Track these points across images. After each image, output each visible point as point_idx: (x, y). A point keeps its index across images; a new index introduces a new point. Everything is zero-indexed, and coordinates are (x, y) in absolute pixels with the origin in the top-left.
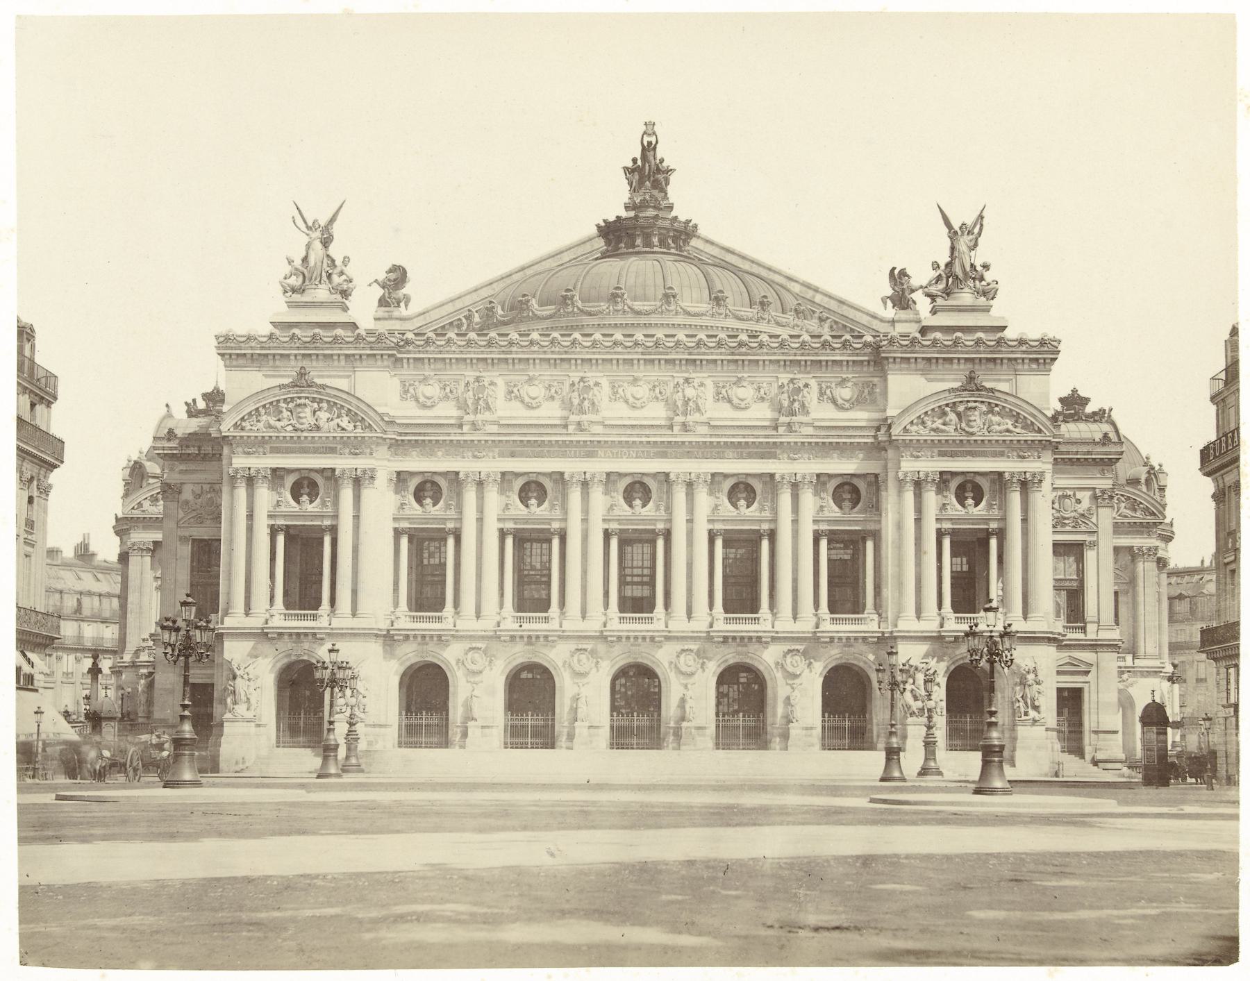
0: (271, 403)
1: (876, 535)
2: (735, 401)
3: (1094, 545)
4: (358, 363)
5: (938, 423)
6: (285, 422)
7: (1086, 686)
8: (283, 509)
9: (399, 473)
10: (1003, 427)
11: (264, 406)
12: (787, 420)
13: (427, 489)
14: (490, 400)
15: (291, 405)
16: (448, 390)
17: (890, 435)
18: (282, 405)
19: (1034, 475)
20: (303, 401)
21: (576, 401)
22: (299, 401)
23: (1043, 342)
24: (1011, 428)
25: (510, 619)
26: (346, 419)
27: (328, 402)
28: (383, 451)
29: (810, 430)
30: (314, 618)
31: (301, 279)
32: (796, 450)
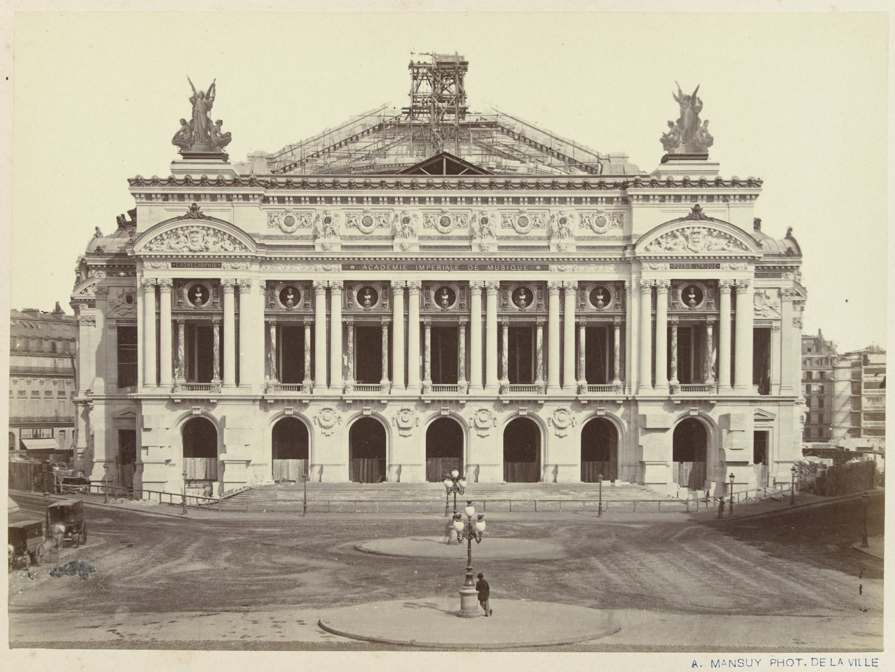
4: (236, 201)
5: (670, 245)
7: (770, 430)
9: (268, 282)
11: (166, 233)
15: (186, 232)
17: (634, 253)
18: (180, 232)
19: (741, 282)
20: (195, 229)
22: (192, 230)
23: (750, 183)
24: (726, 247)
25: (352, 388)
27: (214, 229)
30: (208, 388)
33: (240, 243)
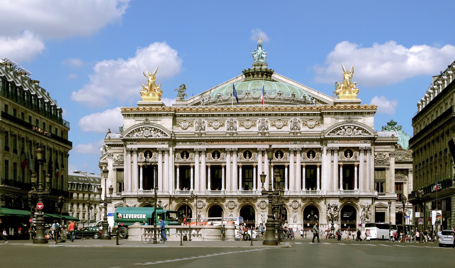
1: (320, 167)
2: (277, 126)
3: (388, 169)
9: (176, 149)
10: (358, 133)
12: (293, 131)
13: (185, 153)
14: (203, 127)
19: (369, 148)
28: (171, 142)
32: (295, 141)
33: (165, 133)
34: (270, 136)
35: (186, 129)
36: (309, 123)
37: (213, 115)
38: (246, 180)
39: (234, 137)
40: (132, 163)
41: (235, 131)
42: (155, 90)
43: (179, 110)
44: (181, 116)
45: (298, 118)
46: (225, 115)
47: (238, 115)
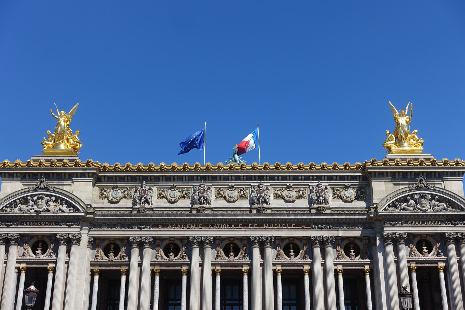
0: (23, 198)
2: (286, 198)
6: (28, 208)
8: (25, 258)
9: (95, 239)
10: (441, 207)
11: (19, 199)
12: (315, 206)
14: (149, 197)
15: (35, 198)
16: (126, 193)
20: (41, 195)
21: (197, 198)
26: (65, 206)
27: (55, 196)
29: (328, 212)
31: (53, 141)
33: (74, 207)
34: (275, 215)
35: (117, 202)
36: (344, 193)
37: (168, 179)
38: (227, 302)
39: (207, 215)
40: (5, 263)
41: (208, 206)
42: (68, 140)
43: (105, 168)
44: (110, 179)
45: (324, 184)
46: (191, 179)
47: (214, 178)
